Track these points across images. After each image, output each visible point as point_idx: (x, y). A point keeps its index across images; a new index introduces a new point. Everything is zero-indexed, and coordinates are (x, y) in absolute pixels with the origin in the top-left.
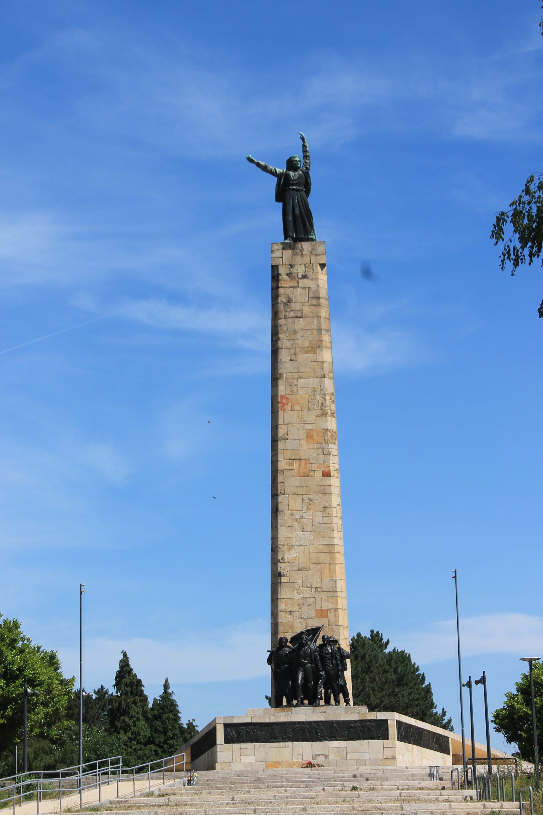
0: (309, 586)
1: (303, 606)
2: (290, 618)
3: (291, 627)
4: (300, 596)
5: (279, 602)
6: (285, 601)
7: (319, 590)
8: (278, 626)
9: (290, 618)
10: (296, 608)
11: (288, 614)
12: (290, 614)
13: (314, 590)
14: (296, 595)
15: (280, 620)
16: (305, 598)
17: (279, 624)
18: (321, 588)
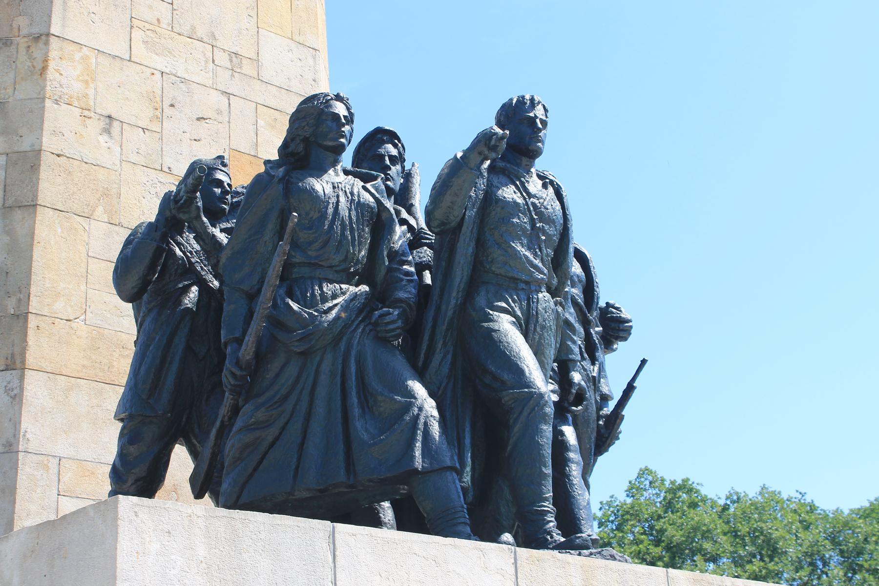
0: (201, 32)
1: (168, 111)
2: (101, 149)
3: (106, 194)
4: (160, 63)
5: (53, 54)
6: (85, 58)
7: (248, 68)
8: (35, 168)
9: (101, 149)
10: (144, 114)
11: (95, 126)
12: (107, 131)
13: (222, 59)
14: (140, 52)
15: (49, 142)
16: (184, 81)
17: (46, 159)
18: (256, 61)
